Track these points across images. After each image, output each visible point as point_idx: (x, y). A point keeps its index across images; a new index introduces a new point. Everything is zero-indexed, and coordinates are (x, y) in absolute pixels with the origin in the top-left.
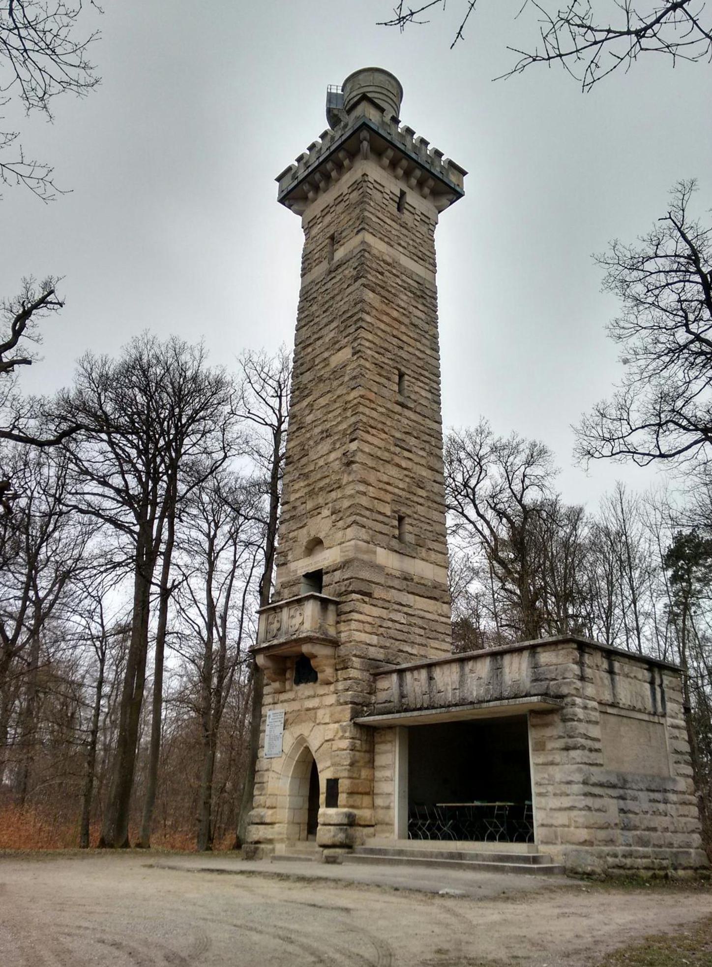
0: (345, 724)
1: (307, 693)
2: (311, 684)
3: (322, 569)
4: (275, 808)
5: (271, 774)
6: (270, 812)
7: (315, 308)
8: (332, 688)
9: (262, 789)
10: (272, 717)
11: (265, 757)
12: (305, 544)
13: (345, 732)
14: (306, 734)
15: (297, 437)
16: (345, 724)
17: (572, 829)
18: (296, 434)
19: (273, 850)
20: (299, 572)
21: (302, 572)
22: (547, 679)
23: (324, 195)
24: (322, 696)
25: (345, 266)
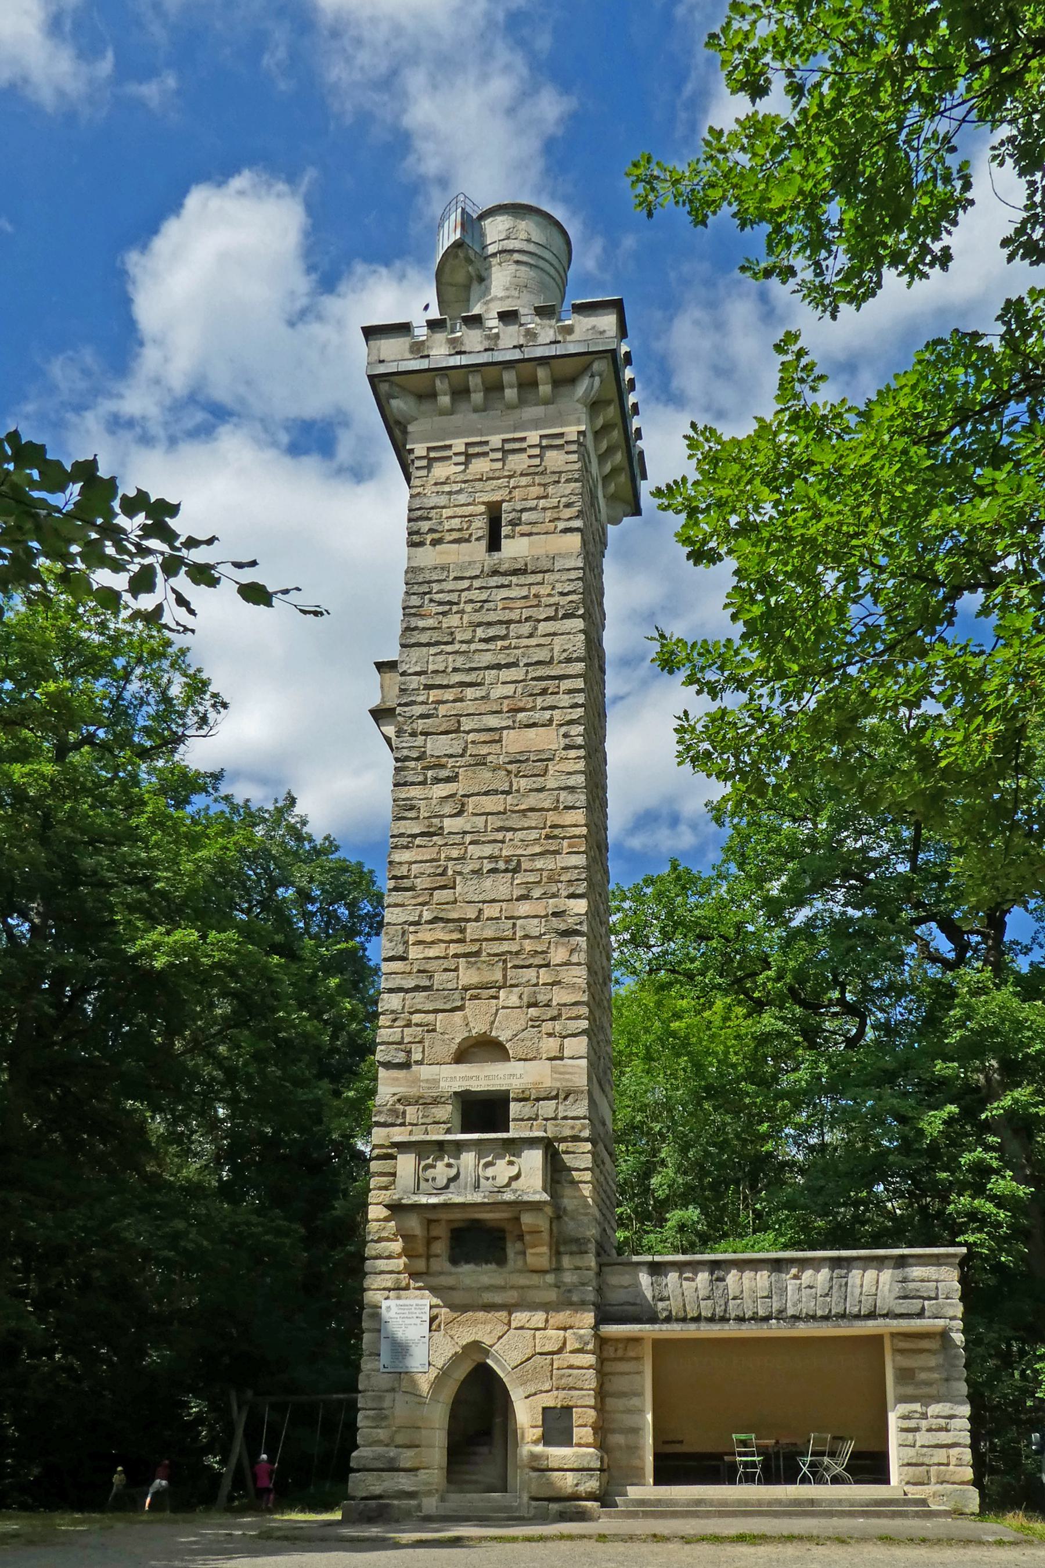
0: (582, 1332)
1: (486, 1280)
2: (492, 1267)
3: (508, 1091)
4: (417, 1446)
5: (398, 1396)
6: (410, 1453)
7: (454, 620)
8: (550, 1278)
9: (381, 1418)
10: (394, 1309)
11: (382, 1370)
12: (458, 1040)
13: (587, 1344)
14: (487, 1341)
15: (418, 846)
16: (582, 1332)
17: (951, 1467)
18: (418, 841)
19: (419, 1507)
20: (442, 1084)
21: (458, 1086)
22: (920, 1297)
23: (475, 416)
24: (522, 1288)
25: (539, 577)
